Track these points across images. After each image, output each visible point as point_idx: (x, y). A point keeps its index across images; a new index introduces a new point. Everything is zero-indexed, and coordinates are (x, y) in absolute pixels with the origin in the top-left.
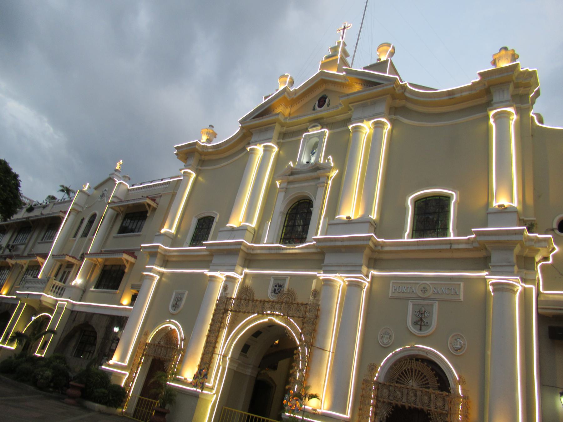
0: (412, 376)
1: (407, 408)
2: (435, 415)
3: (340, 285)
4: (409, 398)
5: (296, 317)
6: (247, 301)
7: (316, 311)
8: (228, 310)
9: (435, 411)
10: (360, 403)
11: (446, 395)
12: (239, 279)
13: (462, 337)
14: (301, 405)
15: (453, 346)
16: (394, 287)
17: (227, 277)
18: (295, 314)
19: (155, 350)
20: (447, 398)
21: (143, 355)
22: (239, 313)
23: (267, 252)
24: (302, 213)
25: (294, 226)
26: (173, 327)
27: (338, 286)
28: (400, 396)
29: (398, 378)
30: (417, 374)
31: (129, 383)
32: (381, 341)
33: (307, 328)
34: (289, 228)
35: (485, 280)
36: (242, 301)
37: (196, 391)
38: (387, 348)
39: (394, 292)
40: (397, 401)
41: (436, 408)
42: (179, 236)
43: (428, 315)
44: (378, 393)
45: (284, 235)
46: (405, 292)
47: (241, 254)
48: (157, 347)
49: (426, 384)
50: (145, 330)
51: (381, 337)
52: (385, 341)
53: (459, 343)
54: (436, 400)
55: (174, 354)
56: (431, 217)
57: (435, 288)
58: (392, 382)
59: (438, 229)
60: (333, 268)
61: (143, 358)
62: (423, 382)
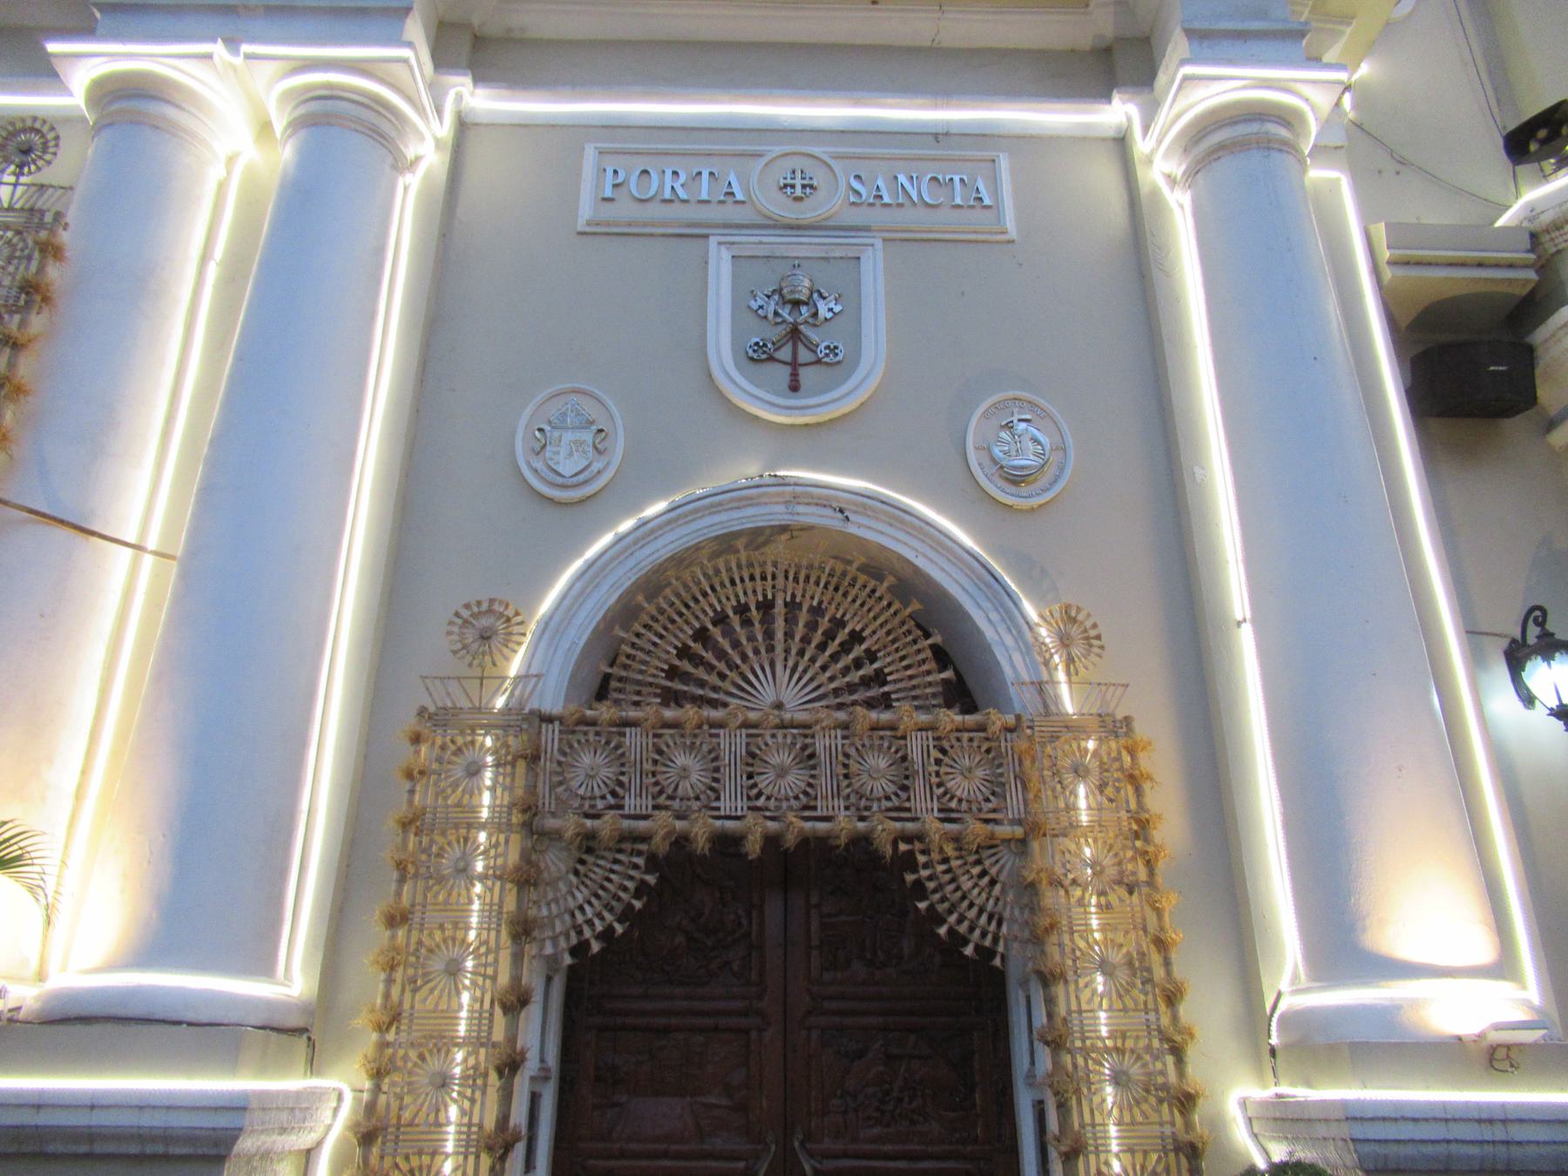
0: (771, 649)
1: (753, 847)
2: (946, 860)
3: (231, 161)
7: (30, 258)
10: (395, 875)
15: (994, 461)
16: (610, 172)
28: (697, 776)
29: (672, 673)
30: (800, 630)
32: (539, 465)
35: (1121, 142)
41: (947, 816)
43: (831, 310)
44: (531, 789)
46: (682, 194)
49: (866, 682)
51: (538, 446)
52: (568, 468)
54: (943, 769)
57: (858, 177)
58: (637, 704)
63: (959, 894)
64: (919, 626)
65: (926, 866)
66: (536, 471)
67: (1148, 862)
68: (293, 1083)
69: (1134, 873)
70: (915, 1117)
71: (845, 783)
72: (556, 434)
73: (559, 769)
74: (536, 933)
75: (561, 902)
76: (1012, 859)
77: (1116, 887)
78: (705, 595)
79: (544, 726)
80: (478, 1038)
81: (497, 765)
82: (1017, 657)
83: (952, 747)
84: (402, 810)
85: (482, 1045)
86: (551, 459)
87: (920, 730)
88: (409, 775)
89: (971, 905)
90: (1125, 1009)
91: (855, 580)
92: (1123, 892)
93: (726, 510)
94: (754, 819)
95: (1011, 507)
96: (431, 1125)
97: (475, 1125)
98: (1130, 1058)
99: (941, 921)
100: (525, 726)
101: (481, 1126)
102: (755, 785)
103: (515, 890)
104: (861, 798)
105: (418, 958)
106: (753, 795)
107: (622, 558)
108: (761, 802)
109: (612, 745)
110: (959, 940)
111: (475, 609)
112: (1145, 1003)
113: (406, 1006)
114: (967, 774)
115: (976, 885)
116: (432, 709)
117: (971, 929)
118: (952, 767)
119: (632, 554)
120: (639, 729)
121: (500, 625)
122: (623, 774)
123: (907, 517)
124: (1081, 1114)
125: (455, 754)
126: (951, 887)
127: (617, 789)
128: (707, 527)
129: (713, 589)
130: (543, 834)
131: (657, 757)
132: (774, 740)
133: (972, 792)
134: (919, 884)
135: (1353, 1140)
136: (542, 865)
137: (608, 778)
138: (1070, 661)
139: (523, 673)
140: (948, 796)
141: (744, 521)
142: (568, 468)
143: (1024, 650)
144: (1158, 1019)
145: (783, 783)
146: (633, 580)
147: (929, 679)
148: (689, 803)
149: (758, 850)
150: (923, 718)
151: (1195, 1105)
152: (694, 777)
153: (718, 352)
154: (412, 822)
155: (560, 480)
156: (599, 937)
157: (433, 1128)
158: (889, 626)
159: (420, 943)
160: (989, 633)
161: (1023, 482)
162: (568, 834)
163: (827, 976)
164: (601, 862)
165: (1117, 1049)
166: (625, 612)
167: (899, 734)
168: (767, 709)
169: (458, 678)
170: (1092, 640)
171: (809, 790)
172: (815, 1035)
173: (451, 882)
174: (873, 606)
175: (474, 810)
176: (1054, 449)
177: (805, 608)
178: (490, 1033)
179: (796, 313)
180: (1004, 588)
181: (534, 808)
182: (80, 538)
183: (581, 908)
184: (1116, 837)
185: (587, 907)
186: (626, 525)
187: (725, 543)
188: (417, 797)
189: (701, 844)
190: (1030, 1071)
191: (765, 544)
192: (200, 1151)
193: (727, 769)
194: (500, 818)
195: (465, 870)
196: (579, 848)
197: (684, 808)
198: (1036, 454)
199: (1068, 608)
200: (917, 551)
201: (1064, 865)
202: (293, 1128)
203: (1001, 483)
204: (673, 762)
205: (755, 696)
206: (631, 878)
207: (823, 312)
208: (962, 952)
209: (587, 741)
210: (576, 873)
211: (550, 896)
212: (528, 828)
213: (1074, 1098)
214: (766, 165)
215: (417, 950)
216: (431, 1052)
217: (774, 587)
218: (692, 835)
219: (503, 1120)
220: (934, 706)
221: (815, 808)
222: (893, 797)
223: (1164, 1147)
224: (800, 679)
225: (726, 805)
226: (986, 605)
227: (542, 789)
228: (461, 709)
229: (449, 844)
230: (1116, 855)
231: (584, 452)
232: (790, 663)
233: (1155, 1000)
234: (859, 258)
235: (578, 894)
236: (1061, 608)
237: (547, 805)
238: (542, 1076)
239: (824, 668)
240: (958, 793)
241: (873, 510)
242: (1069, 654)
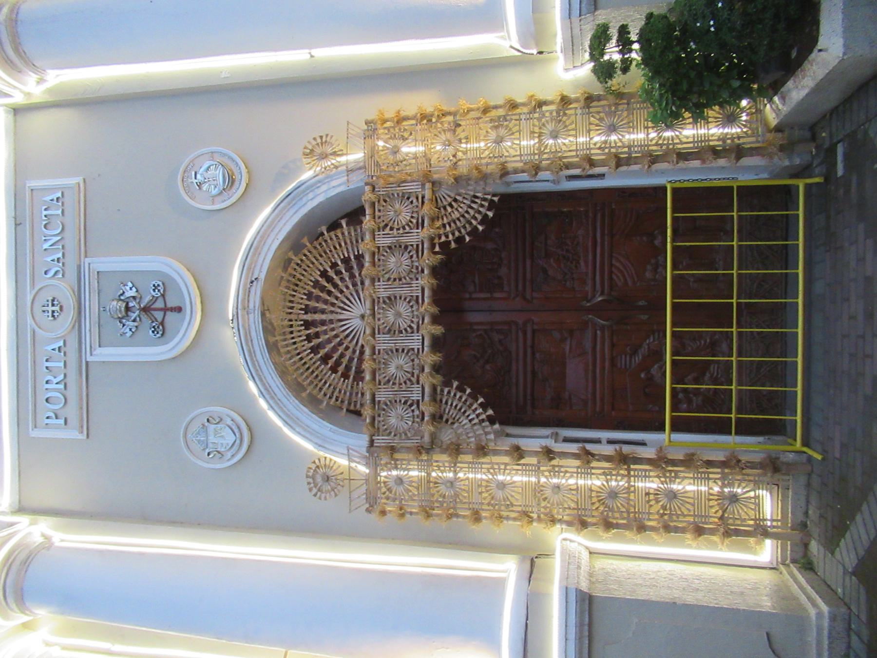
0: (331, 322)
1: (438, 330)
2: (444, 226)
3: (47, 644)
4: (403, 326)
9: (431, 226)
10: (455, 519)
15: (220, 193)
28: (401, 360)
29: (345, 376)
30: (321, 306)
32: (229, 454)
40: (423, 370)
41: (420, 224)
43: (131, 289)
44: (408, 449)
49: (349, 269)
51: (220, 455)
52: (230, 438)
54: (396, 226)
57: (46, 273)
58: (363, 394)
63: (461, 219)
64: (317, 239)
65: (447, 237)
66: (233, 455)
67: (443, 115)
68: (557, 564)
69: (449, 123)
70: (575, 243)
71: (404, 281)
72: (211, 445)
73: (399, 435)
74: (483, 444)
75: (468, 431)
76: (443, 189)
77: (457, 133)
78: (301, 359)
79: (375, 444)
80: (535, 471)
81: (396, 468)
82: (334, 183)
83: (383, 221)
84: (420, 517)
85: (539, 468)
86: (226, 448)
87: (374, 239)
88: (402, 516)
89: (467, 212)
90: (519, 131)
91: (290, 275)
92: (459, 130)
93: (253, 347)
94: (423, 329)
95: (247, 184)
96: (577, 493)
97: (577, 470)
98: (543, 130)
100: (376, 455)
101: (578, 467)
102: (406, 330)
103: (461, 456)
104: (412, 272)
105: (496, 504)
107: (282, 406)
108: (414, 326)
109: (385, 407)
110: (485, 220)
111: (312, 485)
112: (516, 120)
113: (520, 509)
114: (397, 214)
115: (457, 209)
116: (367, 506)
117: (479, 212)
118: (394, 221)
119: (279, 400)
120: (376, 393)
121: (321, 471)
122: (400, 401)
123: (254, 245)
124: (572, 157)
125: (391, 492)
126: (458, 222)
127: (408, 404)
128: (263, 358)
129: (299, 354)
130: (432, 442)
131: (391, 383)
132: (381, 319)
133: (408, 211)
135: (580, 16)
136: (449, 442)
137: (403, 409)
138: (335, 154)
139: (347, 457)
140: (410, 223)
141: (259, 337)
142: (230, 438)
143: (329, 179)
144: (524, 113)
145: (404, 314)
146: (294, 399)
147: (346, 233)
148: (416, 365)
149: (440, 327)
150: (368, 237)
151: (566, 96)
152: (401, 362)
153: (159, 354)
154: (427, 512)
155: (238, 442)
156: (485, 411)
157: (579, 492)
158: (318, 256)
159: (489, 504)
160: (320, 199)
161: (232, 177)
162: (432, 428)
163: (506, 288)
164: (447, 412)
165: (539, 136)
166: (313, 403)
167: (377, 250)
168: (365, 322)
169: (350, 492)
170: (323, 141)
171: (408, 300)
172: (535, 295)
173: (457, 489)
174: (306, 265)
175: (420, 479)
177: (308, 303)
178: (533, 465)
179: (133, 309)
180: (296, 189)
181: (419, 448)
183: (470, 421)
184: (430, 132)
185: (470, 417)
186: (263, 403)
187: (272, 348)
188: (414, 510)
189: (436, 358)
190: (551, 182)
191: (271, 324)
192: (587, 608)
193: (397, 344)
194: (424, 466)
195: (452, 483)
196: (440, 423)
197: (418, 368)
198: (216, 168)
199: (305, 154)
200: (274, 239)
201: (445, 161)
202: (578, 562)
204: (393, 375)
205: (357, 331)
206: (455, 395)
207: (133, 293)
208: (492, 218)
209: (383, 421)
210: (453, 423)
211: (464, 437)
212: (428, 451)
213: (563, 160)
214: (40, 328)
215: (492, 505)
216: (542, 495)
217: (296, 320)
218: (432, 363)
219: (576, 456)
220: (361, 231)
221: (417, 297)
222: (411, 254)
223: (587, 114)
224: (349, 306)
225: (416, 345)
226: (305, 200)
227: (409, 443)
228: (366, 490)
229: (438, 492)
230: (440, 132)
231: (221, 429)
232: (339, 311)
233: (515, 115)
234: (98, 272)
235: (464, 423)
236: (305, 158)
237: (416, 441)
239: (342, 292)
240: (408, 218)
241: (251, 264)
242: (331, 154)
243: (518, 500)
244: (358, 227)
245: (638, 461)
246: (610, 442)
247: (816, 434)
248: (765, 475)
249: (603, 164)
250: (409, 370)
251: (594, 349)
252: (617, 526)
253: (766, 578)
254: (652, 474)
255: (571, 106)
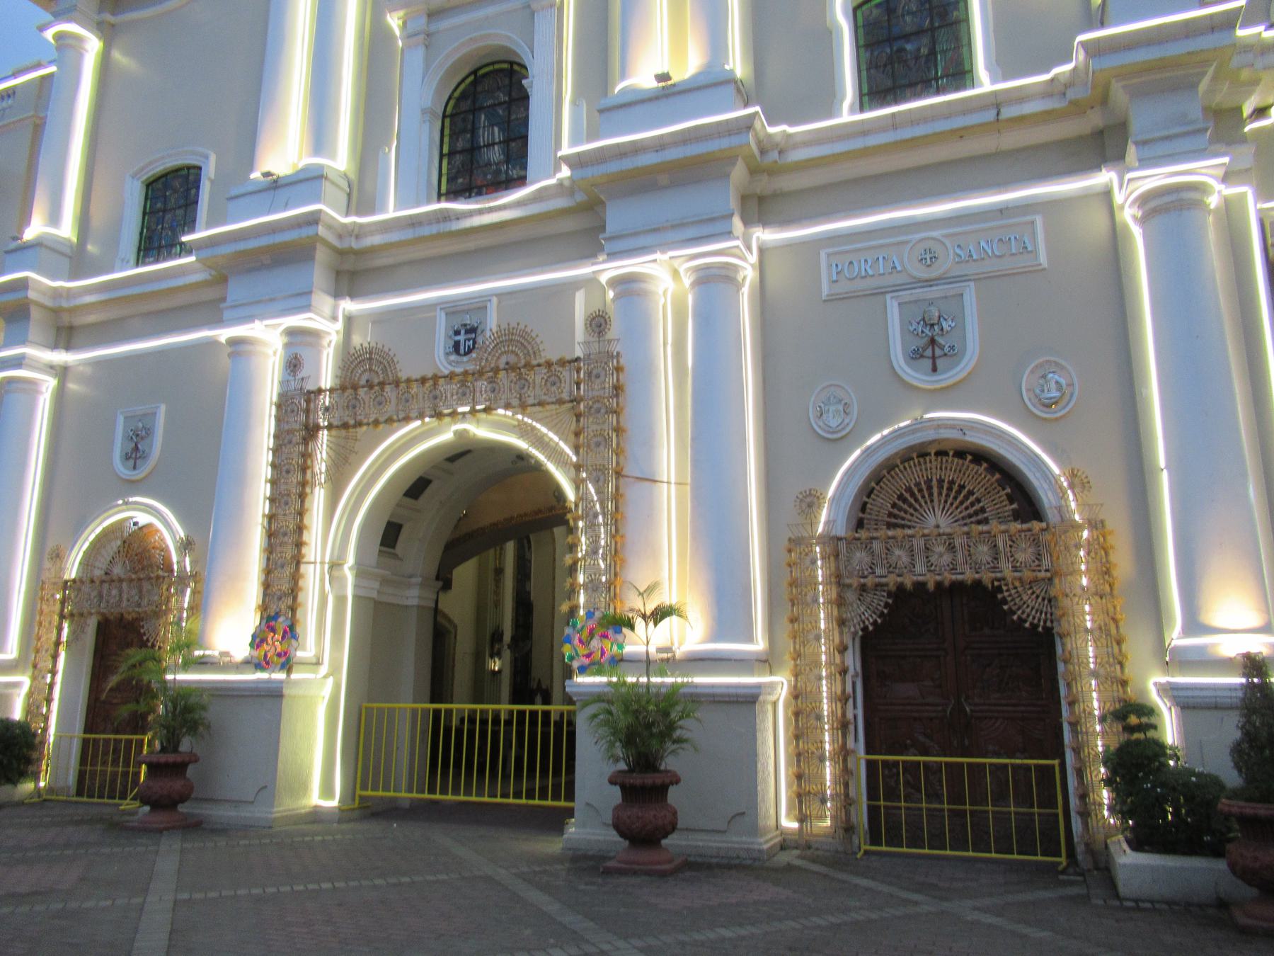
0: (932, 501)
1: (931, 586)
2: (1015, 588)
3: (665, 292)
5: (553, 403)
6: (377, 388)
8: (317, 428)
9: (1015, 578)
10: (790, 604)
11: (1043, 530)
12: (329, 334)
13: (1063, 368)
14: (621, 646)
15: (1036, 396)
17: (292, 333)
18: (545, 394)
19: (100, 596)
20: (1047, 537)
21: (62, 617)
22: (358, 429)
23: (409, 234)
24: (495, 105)
25: (473, 149)
26: (143, 519)
27: (661, 292)
28: (905, 559)
29: (890, 515)
31: (39, 707)
32: (821, 424)
33: (595, 427)
34: (458, 159)
35: (1107, 194)
36: (362, 392)
37: (269, 681)
38: (839, 442)
39: (836, 281)
40: (899, 575)
41: (1015, 569)
42: (90, 247)
43: (950, 326)
44: (838, 568)
45: (448, 181)
46: (870, 272)
47: (321, 254)
48: (106, 586)
49: (976, 513)
50: (51, 545)
51: (819, 414)
52: (834, 423)
53: (1053, 385)
54: (1013, 549)
55: (165, 593)
56: (909, 47)
57: (959, 246)
58: (876, 529)
59: (936, 79)
60: (641, 241)
61: (66, 625)
62: (967, 508)
67: (1110, 585)
82: (1050, 494)
88: (790, 565)
89: (1028, 606)
92: (1097, 598)
99: (1014, 613)
101: (836, 693)
106: (929, 565)
108: (933, 568)
113: (802, 651)
116: (793, 537)
121: (815, 500)
130: (844, 585)
134: (1004, 598)
150: (1003, 527)
153: (896, 356)
156: (871, 624)
159: (803, 629)
172: (969, 658)
175: (816, 577)
176: (1068, 385)
182: (653, 484)
183: (863, 613)
203: (1041, 408)
210: (860, 600)
212: (839, 584)
214: (911, 248)
219: (844, 691)
226: (1033, 469)
227: (842, 567)
232: (941, 507)
234: (962, 295)
238: (856, 675)
239: (957, 508)
243: (808, 650)
244: (1011, 518)
245: (844, 736)
246: (855, 717)
247: (873, 858)
248: (842, 822)
249: (1072, 713)
250: (898, 566)
251: (928, 704)
252: (797, 721)
253: (772, 822)
254: (836, 746)
255: (1120, 686)
